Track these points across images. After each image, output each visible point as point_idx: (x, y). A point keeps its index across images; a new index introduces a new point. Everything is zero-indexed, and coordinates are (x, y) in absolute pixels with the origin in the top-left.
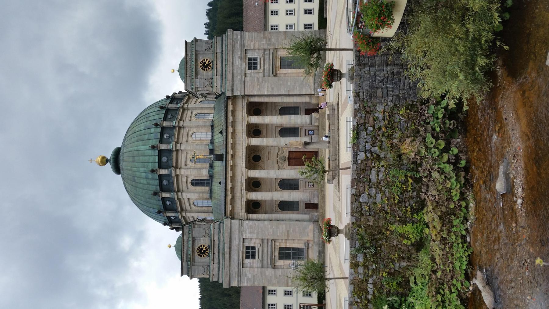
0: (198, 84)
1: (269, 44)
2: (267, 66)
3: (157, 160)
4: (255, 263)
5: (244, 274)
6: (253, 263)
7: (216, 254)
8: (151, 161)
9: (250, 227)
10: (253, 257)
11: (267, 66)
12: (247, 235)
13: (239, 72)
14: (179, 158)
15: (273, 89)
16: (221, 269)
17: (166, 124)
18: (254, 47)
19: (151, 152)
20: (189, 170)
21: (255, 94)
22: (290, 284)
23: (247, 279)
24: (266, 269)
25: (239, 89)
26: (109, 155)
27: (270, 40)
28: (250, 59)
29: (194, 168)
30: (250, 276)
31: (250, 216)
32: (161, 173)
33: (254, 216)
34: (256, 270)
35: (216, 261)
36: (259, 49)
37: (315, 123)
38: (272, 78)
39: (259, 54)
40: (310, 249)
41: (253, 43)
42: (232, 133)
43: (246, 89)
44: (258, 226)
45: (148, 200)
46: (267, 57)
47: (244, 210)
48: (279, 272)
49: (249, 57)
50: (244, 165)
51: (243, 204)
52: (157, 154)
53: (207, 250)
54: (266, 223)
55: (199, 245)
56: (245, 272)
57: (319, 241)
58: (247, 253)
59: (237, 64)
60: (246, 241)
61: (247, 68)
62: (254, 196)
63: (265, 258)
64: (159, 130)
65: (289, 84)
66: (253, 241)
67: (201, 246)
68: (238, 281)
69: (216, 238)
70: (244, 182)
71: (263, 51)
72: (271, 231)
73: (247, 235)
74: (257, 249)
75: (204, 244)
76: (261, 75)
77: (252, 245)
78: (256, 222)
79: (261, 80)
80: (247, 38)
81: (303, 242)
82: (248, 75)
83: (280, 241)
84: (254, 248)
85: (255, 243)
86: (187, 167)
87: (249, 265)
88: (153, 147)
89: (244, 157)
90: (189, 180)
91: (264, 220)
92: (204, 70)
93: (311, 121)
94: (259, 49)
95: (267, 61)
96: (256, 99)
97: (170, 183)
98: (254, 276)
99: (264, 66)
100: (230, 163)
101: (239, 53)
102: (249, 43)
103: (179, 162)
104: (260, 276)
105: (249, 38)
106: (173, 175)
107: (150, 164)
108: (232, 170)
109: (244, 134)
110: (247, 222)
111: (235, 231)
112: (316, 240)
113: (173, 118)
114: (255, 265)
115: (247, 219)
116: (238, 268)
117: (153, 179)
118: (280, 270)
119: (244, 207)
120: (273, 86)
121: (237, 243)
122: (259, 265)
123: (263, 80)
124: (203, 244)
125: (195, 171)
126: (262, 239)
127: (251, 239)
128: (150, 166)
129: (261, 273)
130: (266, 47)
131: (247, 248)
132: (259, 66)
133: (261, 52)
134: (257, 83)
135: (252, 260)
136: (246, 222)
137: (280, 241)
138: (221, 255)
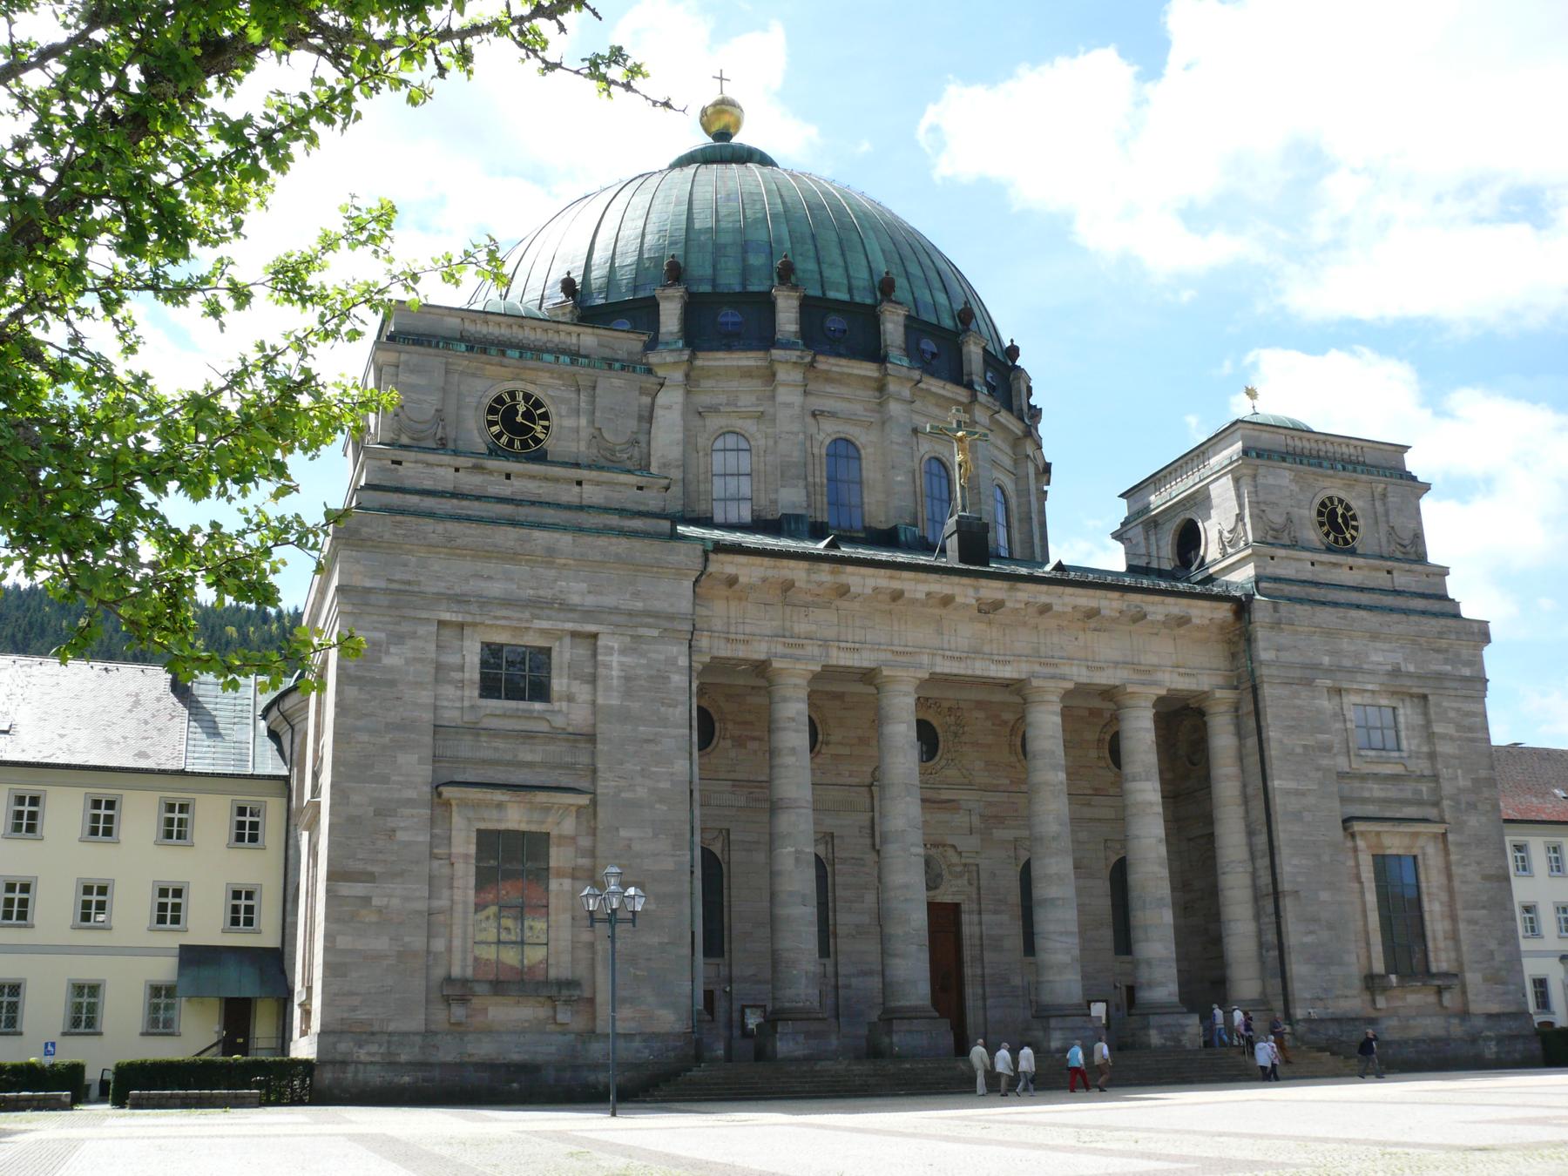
0: (1271, 480)
2: (1376, 790)
3: (832, 294)
4: (461, 698)
5: (405, 628)
6: (461, 684)
7: (505, 489)
8: (827, 272)
9: (660, 678)
10: (489, 687)
11: (1376, 790)
13: (1347, 663)
14: (844, 390)
15: (1297, 816)
16: (429, 503)
17: (973, 351)
18: (1443, 737)
19: (861, 276)
22: (346, 889)
24: (428, 752)
25: (1286, 656)
26: (740, 138)
27: (1472, 806)
30: (393, 659)
32: (781, 303)
34: (425, 696)
35: (469, 482)
37: (1160, 1029)
38: (1338, 811)
39: (1418, 755)
40: (542, 1012)
41: (1451, 730)
42: (1092, 614)
43: (1284, 691)
46: (1408, 790)
47: (725, 651)
48: (412, 830)
51: (758, 651)
52: (858, 299)
53: (525, 445)
56: (414, 635)
57: (595, 1067)
59: (1374, 658)
60: (583, 651)
63: (487, 749)
64: (948, 322)
65: (1325, 896)
66: (582, 691)
67: (545, 416)
68: (369, 590)
69: (592, 494)
70: (864, 660)
71: (1426, 772)
72: (641, 792)
73: (615, 659)
74: (538, 706)
75: (554, 430)
76: (1342, 763)
77: (558, 684)
79: (1325, 762)
81: (581, 972)
83: (585, 842)
84: (541, 691)
85: (570, 699)
86: (810, 420)
87: (452, 659)
88: (886, 288)
89: (980, 668)
92: (1320, 514)
93: (1162, 1009)
94: (1432, 756)
95: (1392, 792)
96: (1223, 740)
97: (730, 341)
98: (392, 683)
99: (1376, 777)
100: (965, 591)
101: (1411, 668)
102: (1452, 714)
103: (829, 389)
107: (812, 266)
109: (1080, 674)
111: (636, 595)
112: (597, 1050)
113: (992, 389)
114: (449, 691)
116: (439, 597)
117: (746, 272)
118: (423, 838)
119: (741, 652)
120: (1307, 816)
121: (575, 599)
122: (450, 715)
126: (591, 738)
128: (806, 266)
129: (401, 727)
130: (1447, 788)
133: (1423, 766)
135: (477, 677)
137: (585, 842)
138: (507, 510)
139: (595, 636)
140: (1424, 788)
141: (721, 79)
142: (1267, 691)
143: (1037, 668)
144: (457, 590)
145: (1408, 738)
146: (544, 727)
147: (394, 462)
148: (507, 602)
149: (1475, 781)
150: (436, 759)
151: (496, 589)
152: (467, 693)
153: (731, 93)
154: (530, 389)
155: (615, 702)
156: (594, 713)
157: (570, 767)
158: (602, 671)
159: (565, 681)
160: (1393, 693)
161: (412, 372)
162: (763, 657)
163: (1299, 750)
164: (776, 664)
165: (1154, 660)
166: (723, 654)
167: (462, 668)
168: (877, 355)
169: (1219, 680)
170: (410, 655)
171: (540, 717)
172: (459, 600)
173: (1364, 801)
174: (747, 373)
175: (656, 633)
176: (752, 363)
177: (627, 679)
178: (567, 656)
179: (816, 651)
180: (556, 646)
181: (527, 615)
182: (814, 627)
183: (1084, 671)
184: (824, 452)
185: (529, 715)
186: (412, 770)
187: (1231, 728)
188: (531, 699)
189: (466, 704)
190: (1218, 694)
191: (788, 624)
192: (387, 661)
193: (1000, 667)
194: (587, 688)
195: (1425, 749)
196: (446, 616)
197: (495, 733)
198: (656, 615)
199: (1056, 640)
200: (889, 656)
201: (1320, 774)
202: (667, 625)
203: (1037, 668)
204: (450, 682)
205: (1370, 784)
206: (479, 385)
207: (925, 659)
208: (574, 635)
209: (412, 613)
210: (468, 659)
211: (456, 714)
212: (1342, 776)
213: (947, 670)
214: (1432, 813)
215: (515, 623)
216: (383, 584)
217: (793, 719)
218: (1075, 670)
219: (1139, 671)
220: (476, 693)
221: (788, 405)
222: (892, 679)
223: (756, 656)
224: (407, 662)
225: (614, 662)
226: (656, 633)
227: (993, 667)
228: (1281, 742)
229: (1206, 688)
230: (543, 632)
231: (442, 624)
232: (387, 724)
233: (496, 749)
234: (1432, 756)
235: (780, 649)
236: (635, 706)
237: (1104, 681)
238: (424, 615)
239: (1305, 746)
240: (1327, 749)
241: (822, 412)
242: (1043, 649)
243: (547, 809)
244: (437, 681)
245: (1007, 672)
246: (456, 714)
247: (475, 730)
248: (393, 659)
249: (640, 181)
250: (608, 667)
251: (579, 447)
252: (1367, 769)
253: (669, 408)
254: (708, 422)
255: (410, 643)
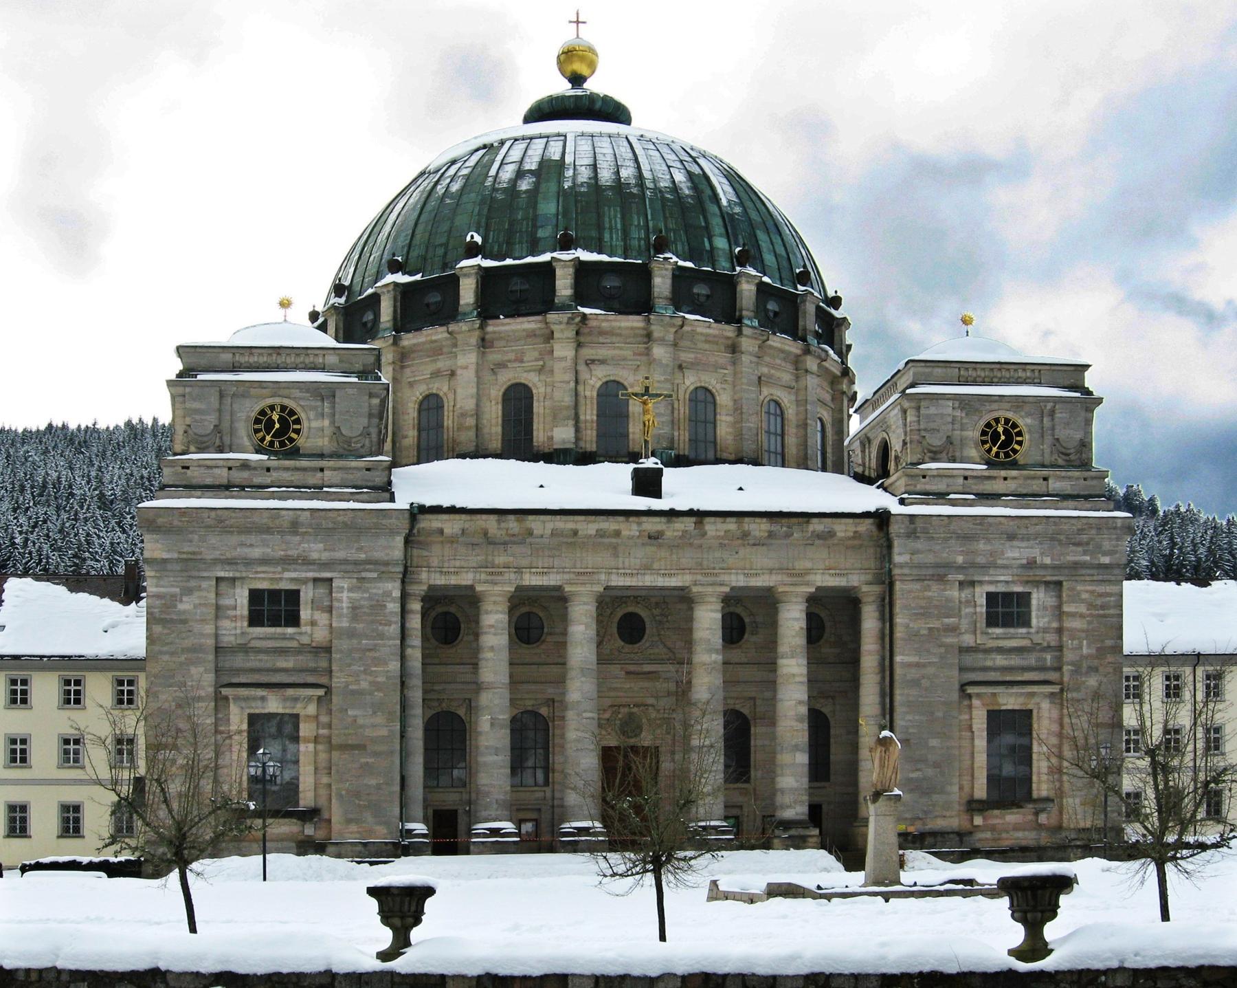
1: (1077, 671)
2: (1000, 660)
4: (235, 628)
5: (193, 583)
9: (379, 606)
10: (255, 619)
11: (1000, 660)
12: (345, 595)
18: (1073, 615)
20: (570, 376)
21: (899, 620)
23: (173, 596)
24: (212, 666)
26: (595, 85)
28: (1024, 599)
29: (576, 395)
30: (185, 605)
31: (416, 606)
33: (415, 622)
34: (209, 629)
36: (1060, 631)
39: (1045, 630)
41: (1083, 609)
44: (381, 636)
45: (445, 227)
47: (440, 580)
49: (1034, 596)
50: (617, 581)
51: (466, 579)
54: (395, 666)
55: (303, 416)
56: (199, 588)
58: (274, 594)
60: (322, 591)
61: (992, 589)
62: (494, 624)
63: (254, 661)
66: (322, 618)
70: (551, 580)
74: (290, 630)
76: (968, 640)
77: (305, 614)
78: (395, 629)
79: (949, 640)
80: (1101, 589)
82: (966, 594)
84: (294, 620)
85: (313, 623)
89: (648, 580)
90: (531, 379)
91: (403, 658)
96: (870, 623)
98: (184, 622)
99: (1000, 650)
102: (1085, 596)
103: (601, 340)
104: (188, 643)
105: (1101, 595)
106: (552, 317)
108: (601, 534)
109: (739, 580)
110: (397, 594)
111: (360, 549)
114: (225, 623)
115: (404, 597)
116: (216, 561)
119: (453, 580)
121: (315, 556)
123: (952, 646)
124: (305, 424)
125: (568, 400)
127: (330, 610)
129: (194, 649)
131: (293, 596)
132: (998, 631)
133: (1051, 639)
134: (936, 624)
135: (246, 612)
136: (394, 588)
139: (331, 580)
140: (1048, 658)
141: (578, 22)
142: (898, 586)
143: (699, 577)
144: (228, 555)
145: (1038, 617)
146: (294, 644)
147: (183, 468)
148: (264, 561)
149: (1098, 649)
150: (217, 671)
151: (256, 553)
152: (239, 624)
153: (589, 35)
154: (286, 402)
155: (345, 624)
156: (331, 633)
157: (313, 671)
158: (335, 604)
159: (309, 612)
160: (1027, 582)
161: (194, 400)
162: (469, 583)
163: (925, 632)
164: (479, 588)
165: (809, 565)
166: (438, 582)
167: (235, 608)
168: (643, 305)
169: (869, 577)
170: (197, 602)
171: (292, 638)
172: (231, 562)
173: (985, 669)
174: (532, 334)
175: (375, 575)
176: (533, 326)
177: (354, 608)
178: (311, 594)
179: (513, 576)
180: (303, 589)
181: (279, 569)
182: (511, 559)
183: (741, 577)
184: (595, 394)
185: (284, 637)
186: (203, 678)
187: (876, 614)
188: (287, 625)
189: (238, 631)
190: (865, 588)
191: (490, 558)
192: (181, 607)
193: (667, 579)
194: (326, 616)
195: (1055, 625)
196: (222, 574)
197: (259, 651)
198: (375, 562)
199: (718, 554)
200: (572, 576)
201: (942, 650)
202: (383, 569)
203: (699, 577)
204: (228, 618)
205: (993, 656)
206: (247, 403)
207: (603, 577)
208: (315, 580)
209: (196, 574)
210: (239, 601)
211: (232, 638)
212: (964, 650)
213: (621, 584)
214: (1052, 676)
215: (271, 576)
216: (176, 556)
217: (492, 626)
218: (733, 577)
219: (792, 575)
220: (246, 624)
221: (564, 359)
222: (574, 594)
223: (464, 583)
224: (195, 607)
225: (345, 596)
226: (375, 575)
227: (660, 579)
228: (907, 626)
229: (856, 584)
230: (292, 580)
231: (218, 579)
232: (183, 650)
233: (261, 660)
234: (1060, 631)
235: (483, 576)
236: (360, 626)
237: (759, 584)
238: (205, 574)
239: (930, 629)
240: (953, 629)
241: (593, 361)
242: (705, 563)
243: (296, 699)
244: (217, 617)
245: (673, 582)
246: (232, 638)
247: (245, 649)
248: (185, 605)
249: (481, 152)
250: (340, 601)
251: (323, 443)
252: (992, 644)
253: (466, 368)
254: (499, 377)
255: (197, 594)
